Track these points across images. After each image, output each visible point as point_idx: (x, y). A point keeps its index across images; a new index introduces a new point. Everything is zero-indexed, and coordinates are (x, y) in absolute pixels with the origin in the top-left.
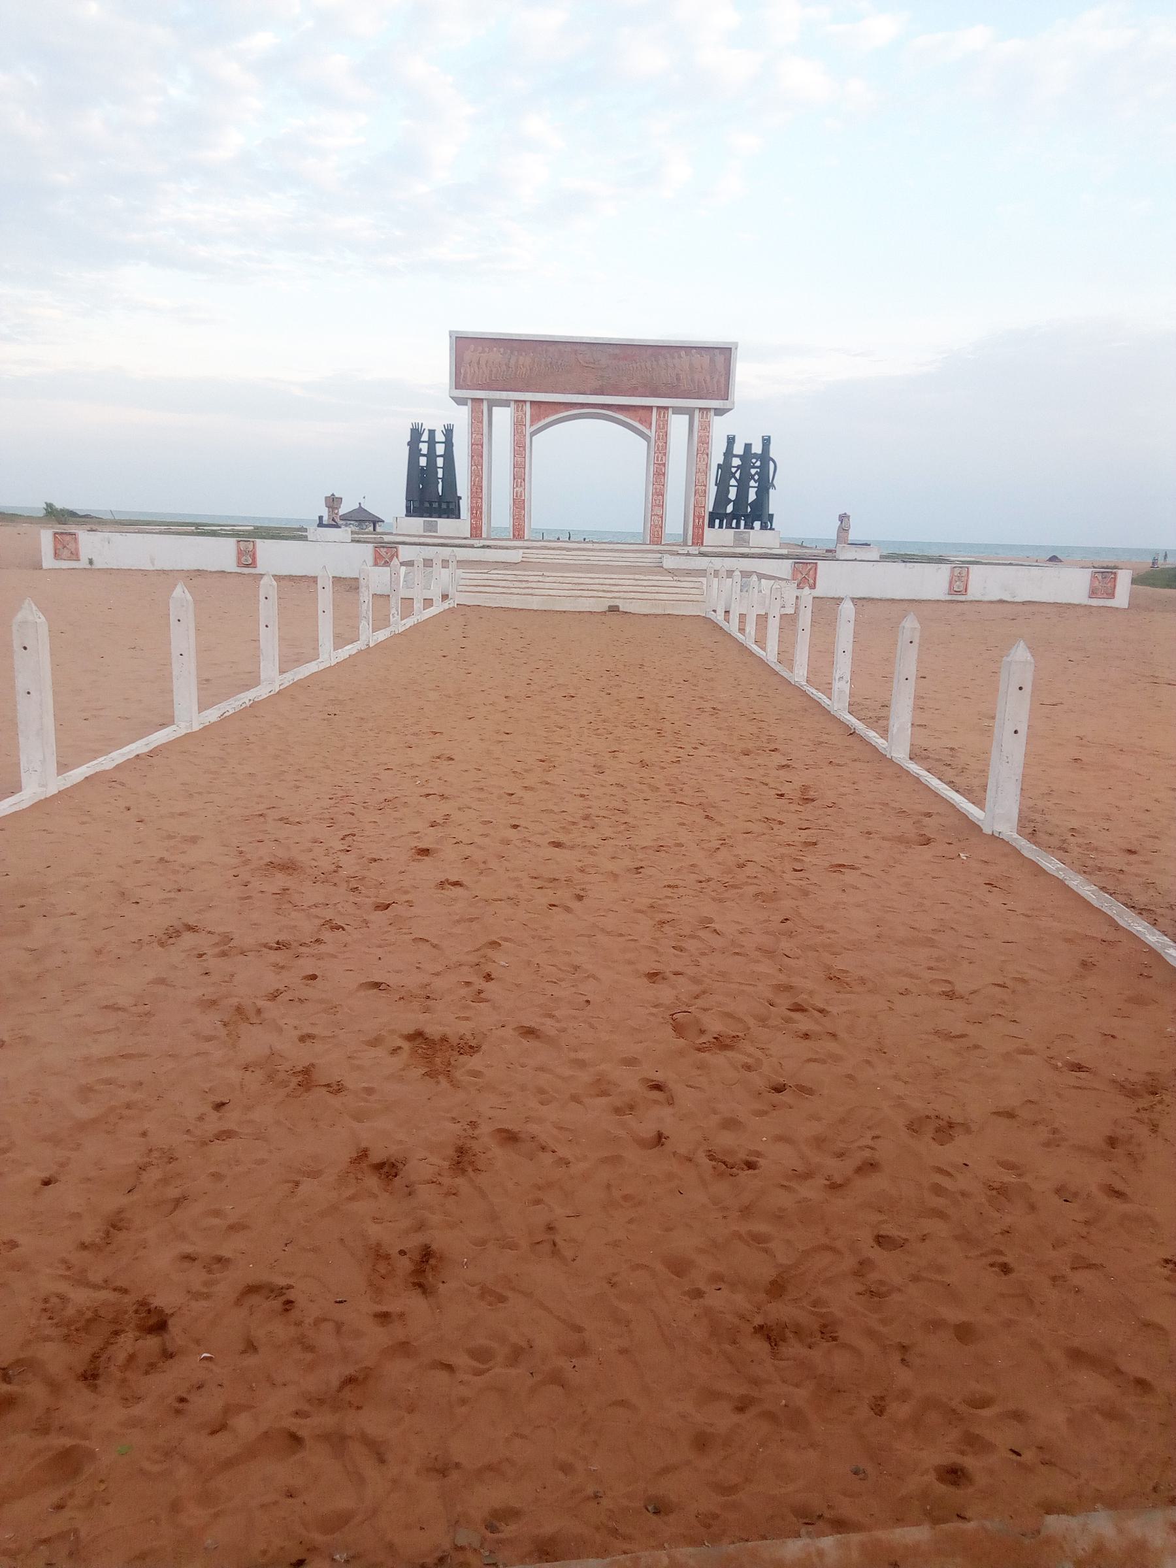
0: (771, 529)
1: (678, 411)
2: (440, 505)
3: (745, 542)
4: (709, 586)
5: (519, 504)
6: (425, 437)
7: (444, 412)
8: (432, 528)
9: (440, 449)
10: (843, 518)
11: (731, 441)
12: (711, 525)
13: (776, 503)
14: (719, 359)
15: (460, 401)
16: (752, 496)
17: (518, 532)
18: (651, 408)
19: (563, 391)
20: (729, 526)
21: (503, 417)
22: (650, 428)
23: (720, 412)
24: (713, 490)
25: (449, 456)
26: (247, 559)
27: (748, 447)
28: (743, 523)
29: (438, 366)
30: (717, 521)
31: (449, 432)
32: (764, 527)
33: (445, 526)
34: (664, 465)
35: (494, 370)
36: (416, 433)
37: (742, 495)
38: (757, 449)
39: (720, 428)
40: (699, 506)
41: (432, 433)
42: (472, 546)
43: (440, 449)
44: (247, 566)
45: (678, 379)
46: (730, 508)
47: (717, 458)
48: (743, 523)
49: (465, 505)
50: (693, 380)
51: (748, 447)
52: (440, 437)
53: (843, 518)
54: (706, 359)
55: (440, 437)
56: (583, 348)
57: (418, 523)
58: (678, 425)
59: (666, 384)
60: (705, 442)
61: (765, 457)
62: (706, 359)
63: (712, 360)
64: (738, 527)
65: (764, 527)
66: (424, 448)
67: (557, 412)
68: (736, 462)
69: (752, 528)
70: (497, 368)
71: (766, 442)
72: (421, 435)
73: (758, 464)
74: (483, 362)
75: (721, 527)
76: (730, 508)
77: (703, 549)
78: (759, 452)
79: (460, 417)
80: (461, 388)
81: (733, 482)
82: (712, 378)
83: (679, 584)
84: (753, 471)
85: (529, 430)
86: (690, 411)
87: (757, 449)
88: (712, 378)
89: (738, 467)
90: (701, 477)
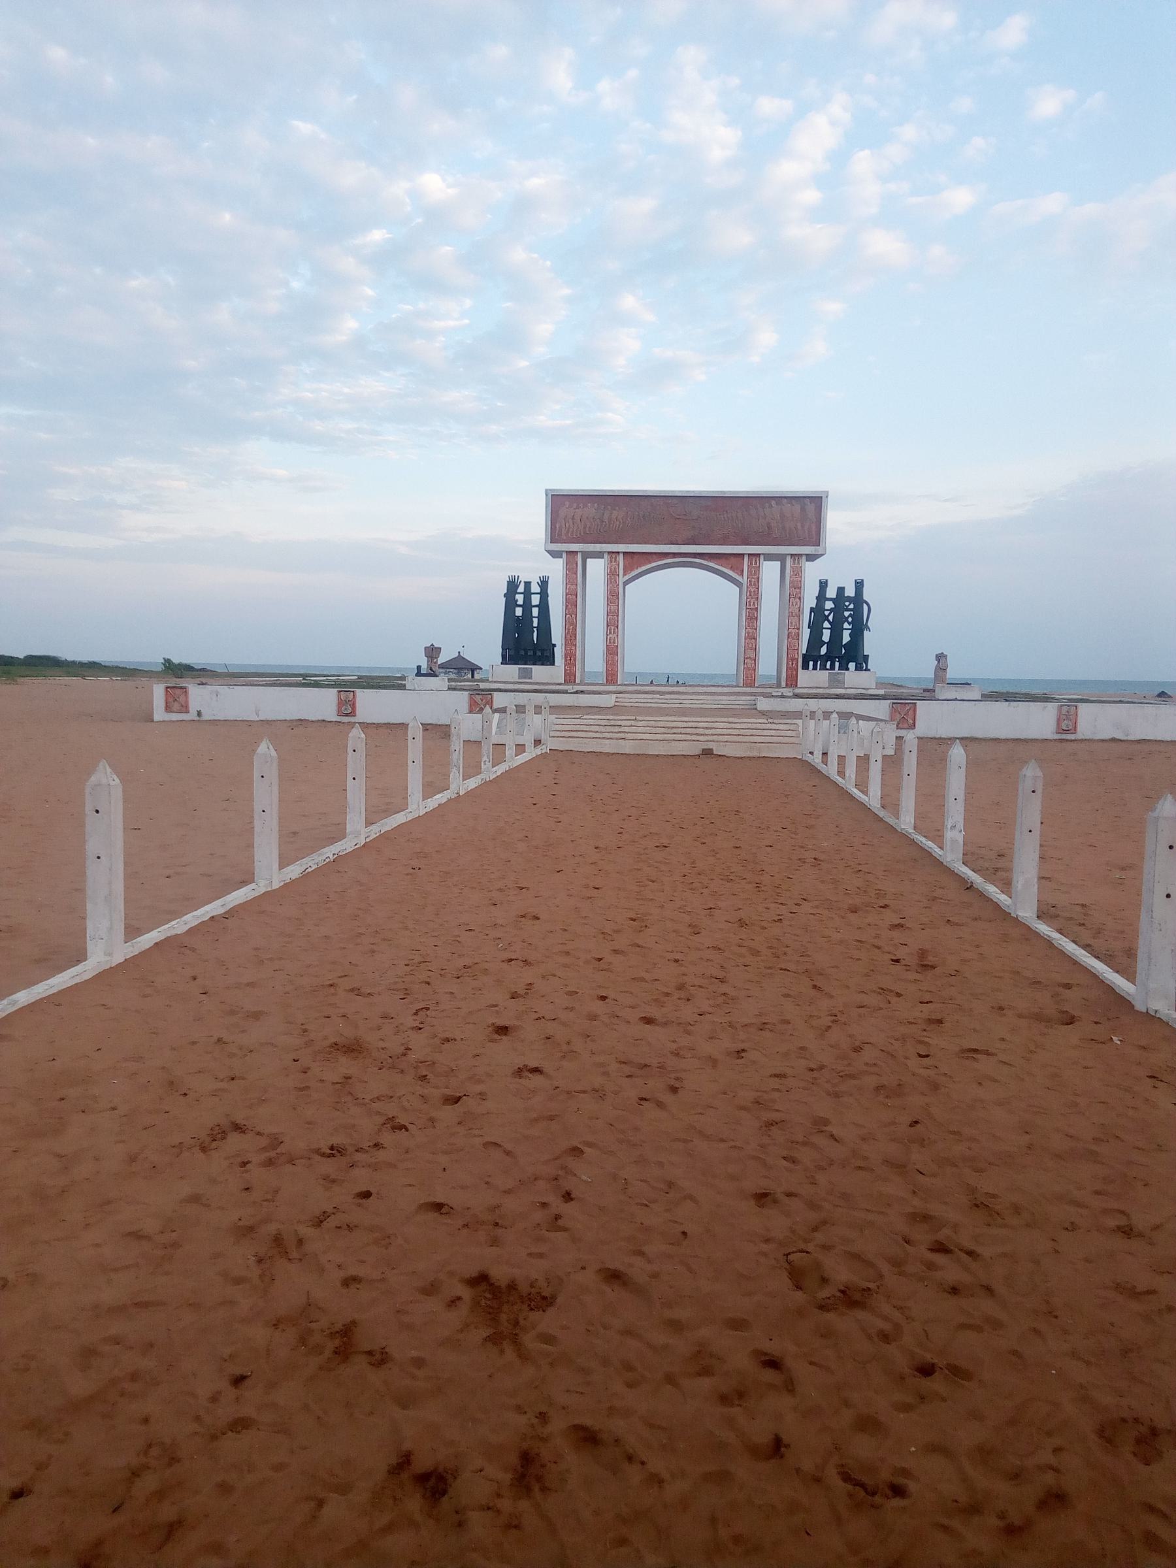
0: (867, 670)
1: (769, 557)
2: (535, 653)
3: (840, 683)
4: (805, 728)
5: (612, 651)
6: (521, 589)
7: (539, 564)
8: (526, 675)
9: (535, 600)
10: (941, 658)
11: (823, 585)
12: (805, 667)
13: (871, 643)
14: (811, 508)
15: (555, 554)
16: (846, 638)
17: (611, 677)
20: (824, 668)
21: (596, 569)
23: (811, 558)
24: (806, 633)
25: (544, 606)
26: (347, 708)
27: (841, 590)
28: (837, 664)
29: (533, 522)
30: (811, 663)
31: (544, 583)
32: (859, 668)
33: (539, 672)
36: (512, 585)
37: (836, 636)
38: (850, 592)
39: (812, 574)
40: (792, 649)
41: (528, 584)
42: (566, 692)
43: (535, 600)
44: (347, 715)
45: (769, 528)
46: (824, 650)
47: (810, 601)
48: (837, 664)
49: (559, 653)
50: (784, 528)
51: (841, 590)
52: (535, 588)
53: (941, 658)
55: (535, 588)
56: (675, 501)
57: (513, 670)
58: (770, 572)
60: (797, 586)
61: (858, 600)
62: (797, 507)
63: (803, 509)
64: (833, 668)
65: (859, 668)
66: (520, 599)
68: (829, 605)
69: (848, 669)
70: (591, 522)
71: (859, 585)
72: (518, 587)
73: (852, 606)
74: (577, 518)
75: (815, 668)
76: (824, 650)
77: (797, 691)
78: (853, 595)
79: (556, 570)
81: (826, 625)
83: (774, 726)
84: (847, 614)
85: (622, 579)
86: (781, 558)
87: (850, 592)
88: (802, 527)
89: (831, 610)
90: (794, 620)
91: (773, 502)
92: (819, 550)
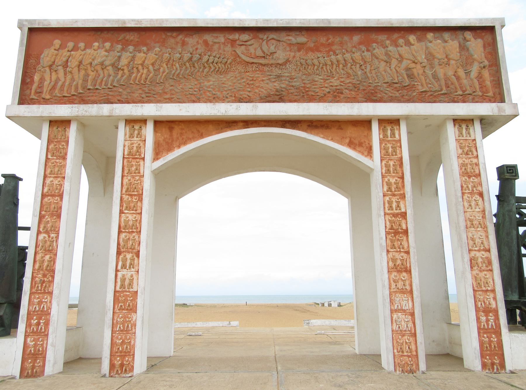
18: (364, 123)
19: (214, 99)
22: (369, 152)
23: (489, 125)
34: (404, 215)
35: (92, 74)
45: (411, 76)
50: (435, 76)
54: (453, 44)
56: (245, 37)
59: (390, 84)
60: (471, 173)
67: (202, 136)
80: (32, 102)
82: (468, 73)
85: (149, 166)
88: (468, 73)
91: (412, 38)
92: (506, 109)
